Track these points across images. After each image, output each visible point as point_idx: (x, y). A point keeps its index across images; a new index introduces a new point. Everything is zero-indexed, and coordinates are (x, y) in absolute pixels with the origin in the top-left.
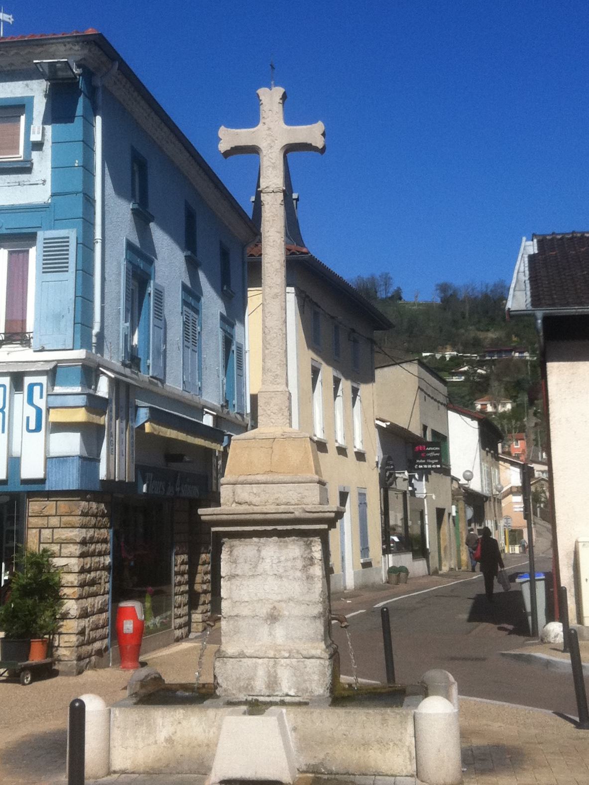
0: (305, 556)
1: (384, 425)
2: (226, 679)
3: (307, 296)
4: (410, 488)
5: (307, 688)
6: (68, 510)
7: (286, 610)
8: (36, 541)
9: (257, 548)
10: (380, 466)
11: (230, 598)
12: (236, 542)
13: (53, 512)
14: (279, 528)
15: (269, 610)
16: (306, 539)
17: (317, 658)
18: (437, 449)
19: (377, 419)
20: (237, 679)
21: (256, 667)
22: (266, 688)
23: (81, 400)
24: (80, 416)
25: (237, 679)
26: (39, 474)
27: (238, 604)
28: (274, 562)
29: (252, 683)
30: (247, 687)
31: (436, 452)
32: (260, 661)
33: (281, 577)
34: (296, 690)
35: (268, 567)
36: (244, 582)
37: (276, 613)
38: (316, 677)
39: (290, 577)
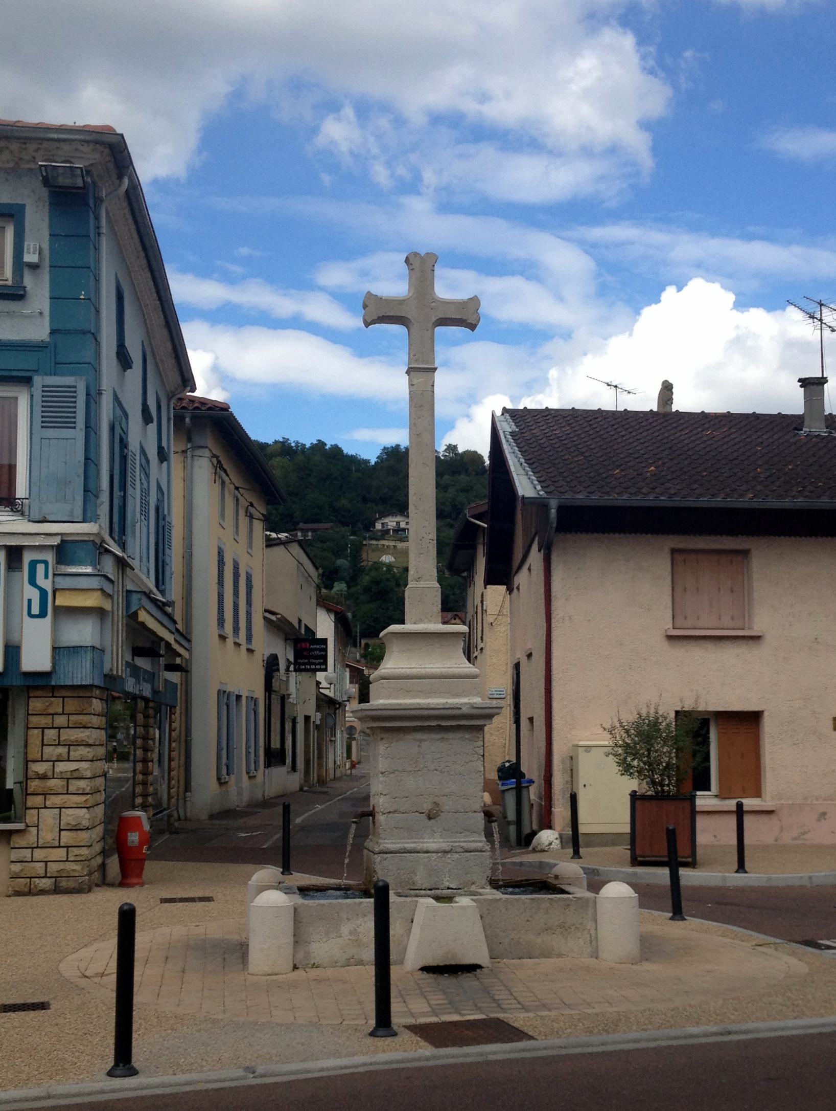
1: (273, 618)
3: (219, 462)
7: (448, 804)
8: (39, 743)
13: (60, 711)
26: (44, 665)
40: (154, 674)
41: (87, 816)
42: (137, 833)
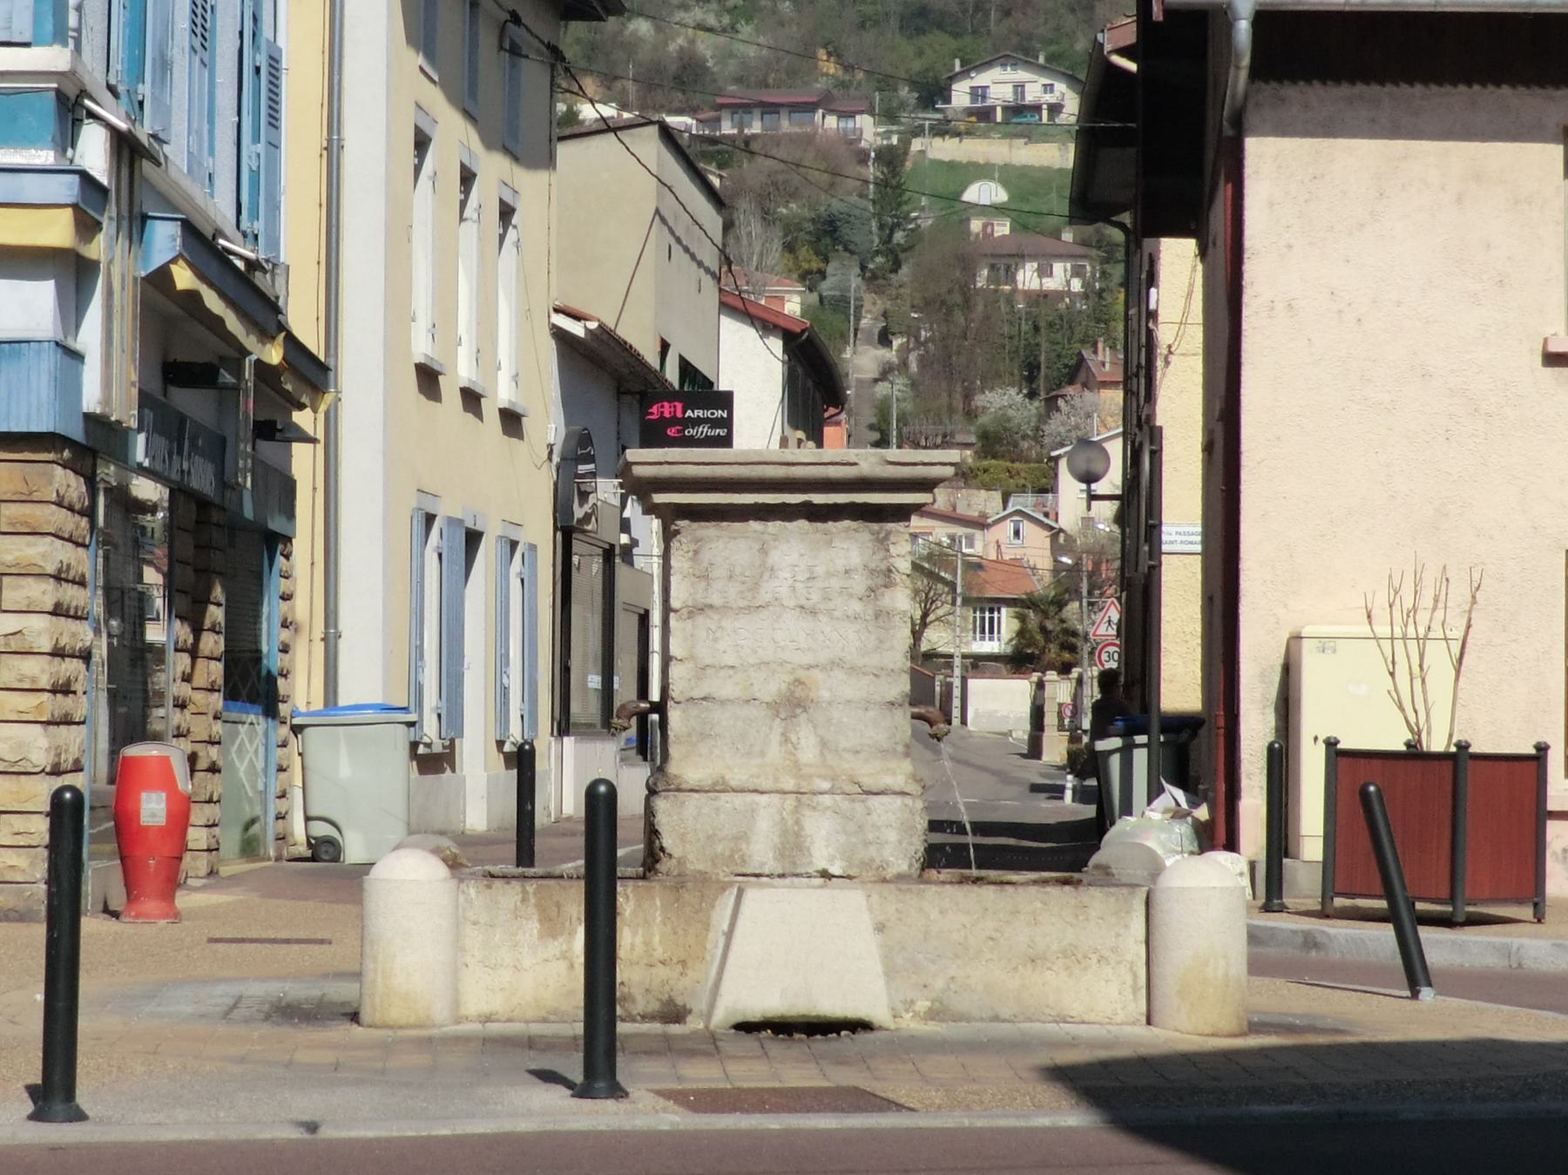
0: (872, 565)
1: (577, 329)
2: (683, 837)
4: (624, 539)
5: (872, 860)
6: (22, 487)
7: (825, 687)
9: (757, 547)
10: (556, 459)
11: (692, 657)
12: (708, 530)
14: (819, 499)
15: (784, 686)
16: (875, 526)
17: (895, 793)
18: (719, 413)
19: (557, 311)
20: (709, 837)
21: (753, 811)
22: (775, 859)
23: (65, 189)
24: (56, 231)
25: (709, 837)
27: (709, 671)
28: (800, 578)
29: (744, 846)
30: (732, 856)
31: (715, 423)
32: (764, 799)
33: (813, 613)
34: (844, 864)
35: (784, 591)
36: (724, 623)
37: (799, 692)
38: (892, 836)
39: (836, 614)
40: (223, 441)
41: (43, 742)
42: (164, 795)
